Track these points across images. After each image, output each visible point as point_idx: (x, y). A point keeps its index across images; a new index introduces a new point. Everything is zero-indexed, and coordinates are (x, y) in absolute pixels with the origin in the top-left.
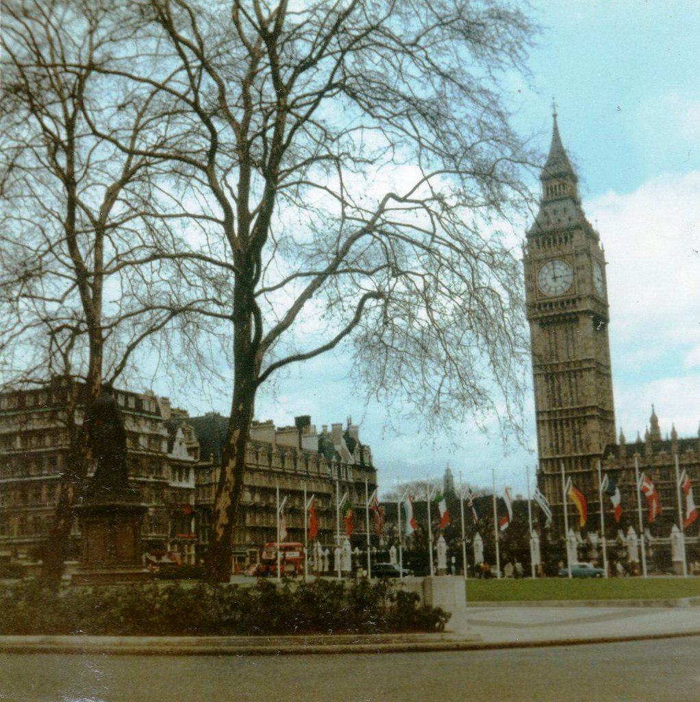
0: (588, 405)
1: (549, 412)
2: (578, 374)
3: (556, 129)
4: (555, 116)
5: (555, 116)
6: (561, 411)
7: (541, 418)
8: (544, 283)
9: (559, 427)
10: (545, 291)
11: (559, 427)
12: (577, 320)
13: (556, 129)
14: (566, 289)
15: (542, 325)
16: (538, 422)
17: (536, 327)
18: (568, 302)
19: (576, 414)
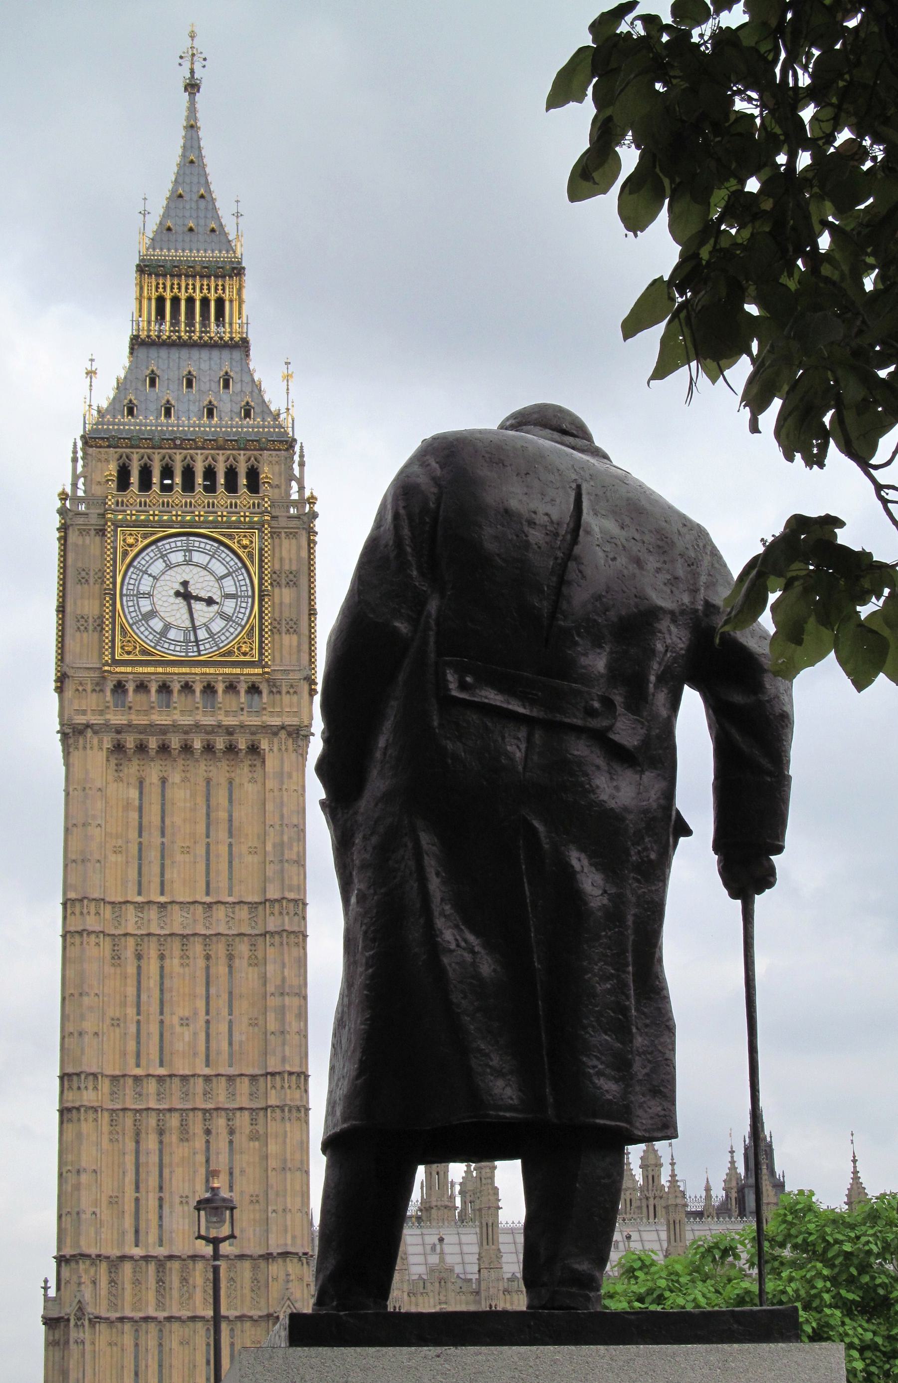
0: (273, 1065)
1: (114, 1078)
2: (243, 948)
3: (192, 127)
4: (192, 87)
5: (192, 87)
6: (160, 1079)
7: (89, 1097)
8: (145, 606)
9: (151, 1142)
10: (144, 635)
11: (151, 1142)
12: (254, 749)
13: (192, 127)
14: (225, 642)
15: (119, 748)
16: (65, 1112)
17: (96, 757)
18: (231, 687)
19: (221, 1098)
